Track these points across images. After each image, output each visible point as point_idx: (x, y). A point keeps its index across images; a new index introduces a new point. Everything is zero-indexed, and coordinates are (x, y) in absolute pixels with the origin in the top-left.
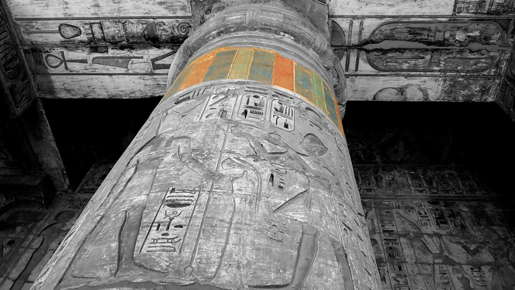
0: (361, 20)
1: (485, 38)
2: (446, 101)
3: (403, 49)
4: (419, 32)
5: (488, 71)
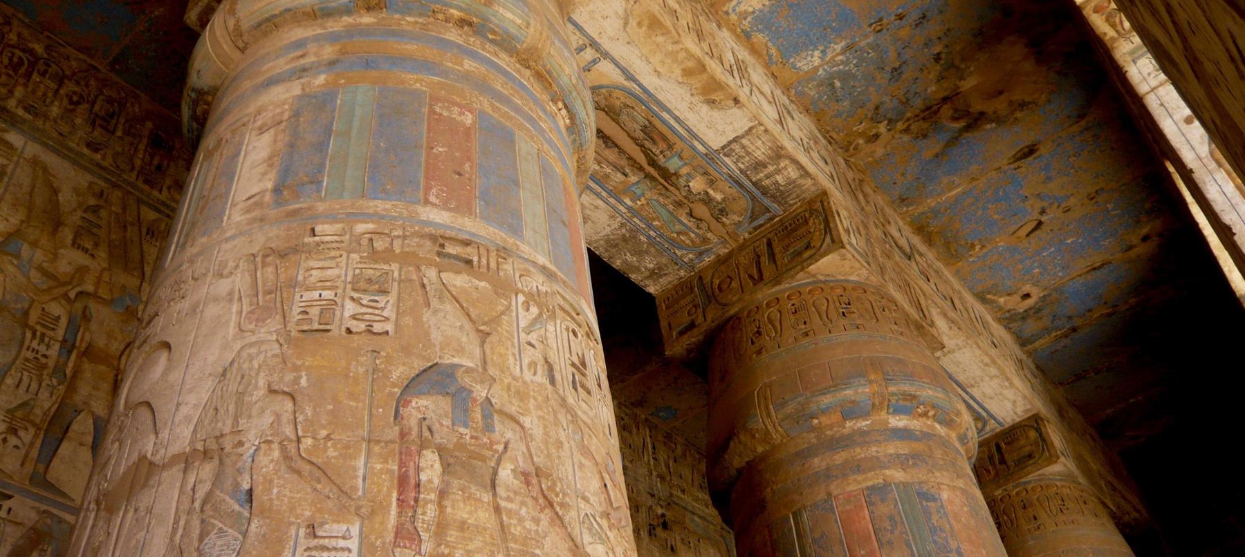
0: (599, 56)
1: (721, 211)
2: (597, 252)
3: (614, 143)
4: (656, 137)
5: (685, 252)
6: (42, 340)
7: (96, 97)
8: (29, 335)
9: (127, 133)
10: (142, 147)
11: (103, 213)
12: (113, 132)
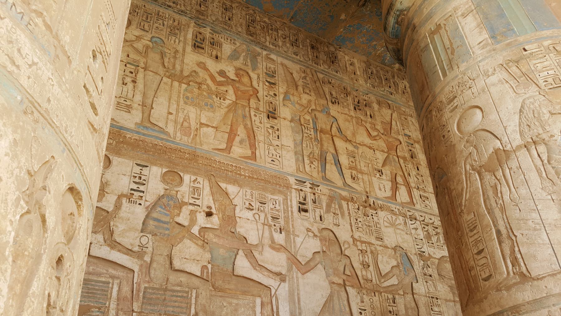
6: (308, 129)
7: (289, 34)
8: (303, 128)
9: (303, 46)
10: (309, 50)
11: (308, 78)
12: (299, 47)
